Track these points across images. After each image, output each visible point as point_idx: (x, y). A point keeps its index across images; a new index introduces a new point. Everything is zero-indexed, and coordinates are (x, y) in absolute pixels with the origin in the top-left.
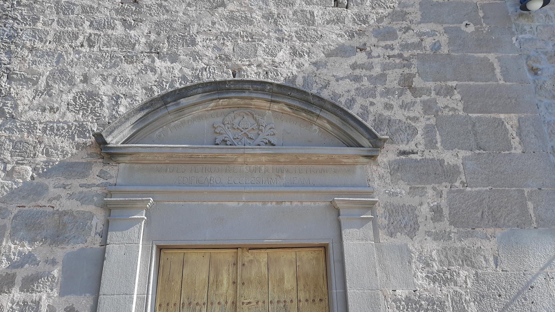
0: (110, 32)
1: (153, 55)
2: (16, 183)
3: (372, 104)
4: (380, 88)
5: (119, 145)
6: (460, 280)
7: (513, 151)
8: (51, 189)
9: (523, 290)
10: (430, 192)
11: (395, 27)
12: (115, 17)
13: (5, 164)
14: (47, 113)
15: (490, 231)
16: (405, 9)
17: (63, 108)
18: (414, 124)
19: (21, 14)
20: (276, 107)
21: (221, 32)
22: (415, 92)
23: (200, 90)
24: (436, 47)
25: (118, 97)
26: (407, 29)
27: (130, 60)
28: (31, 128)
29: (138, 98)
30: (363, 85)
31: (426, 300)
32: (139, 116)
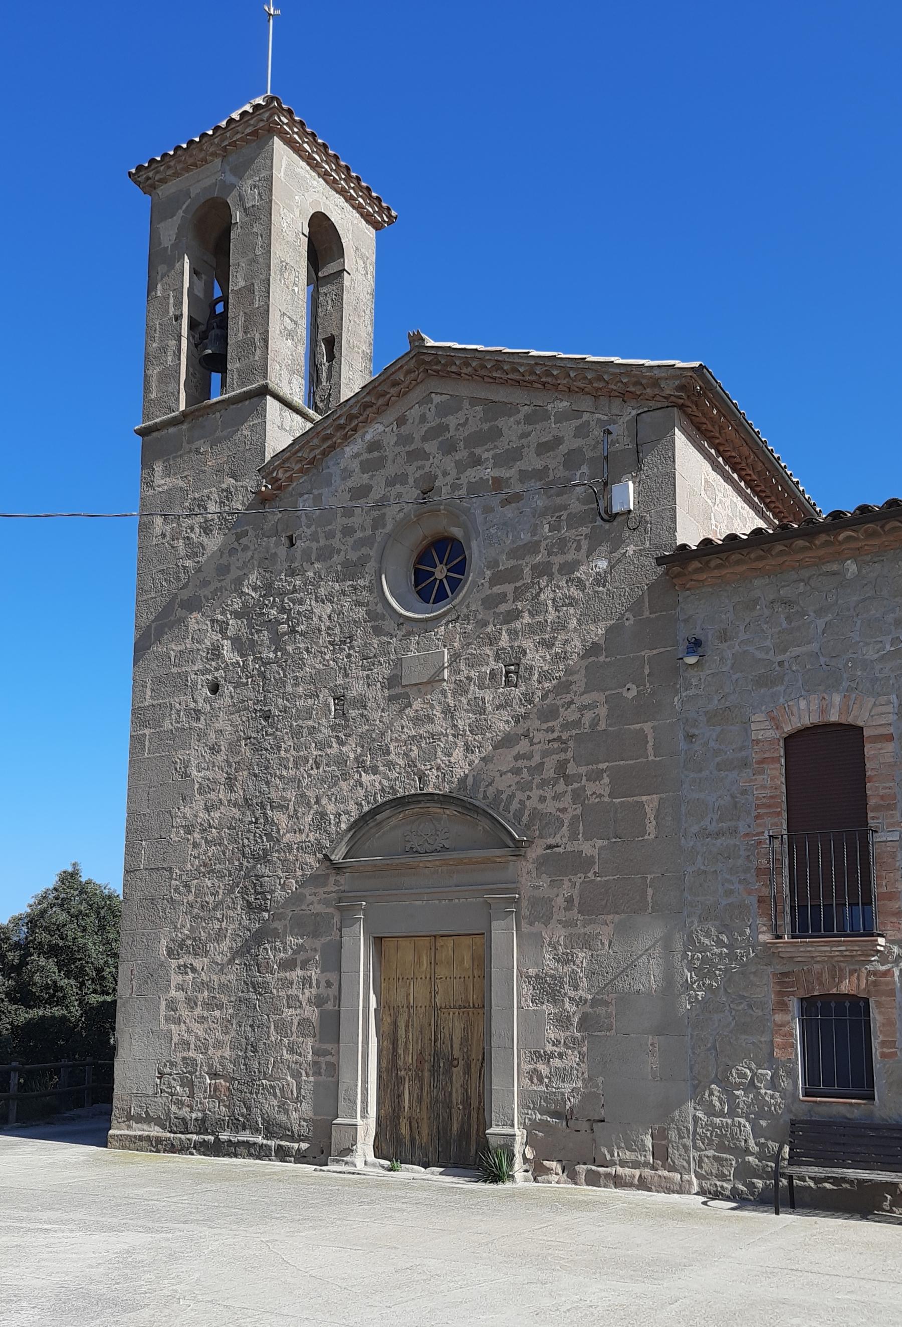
0: (329, 751)
1: (360, 769)
2: (288, 893)
3: (529, 798)
4: (537, 780)
5: (340, 861)
6: (578, 962)
7: (646, 837)
8: (308, 897)
9: (627, 968)
10: (567, 884)
11: (559, 703)
12: (331, 734)
13: (280, 878)
14: (297, 835)
15: (610, 917)
16: (570, 678)
17: (307, 830)
18: (561, 816)
19: (270, 744)
20: (448, 812)
21: (409, 736)
22: (568, 780)
23: (387, 807)
24: (595, 722)
25: (340, 815)
26: (571, 702)
27: (345, 776)
28: (289, 847)
29: (352, 814)
30: (522, 778)
31: (551, 976)
32: (349, 835)
